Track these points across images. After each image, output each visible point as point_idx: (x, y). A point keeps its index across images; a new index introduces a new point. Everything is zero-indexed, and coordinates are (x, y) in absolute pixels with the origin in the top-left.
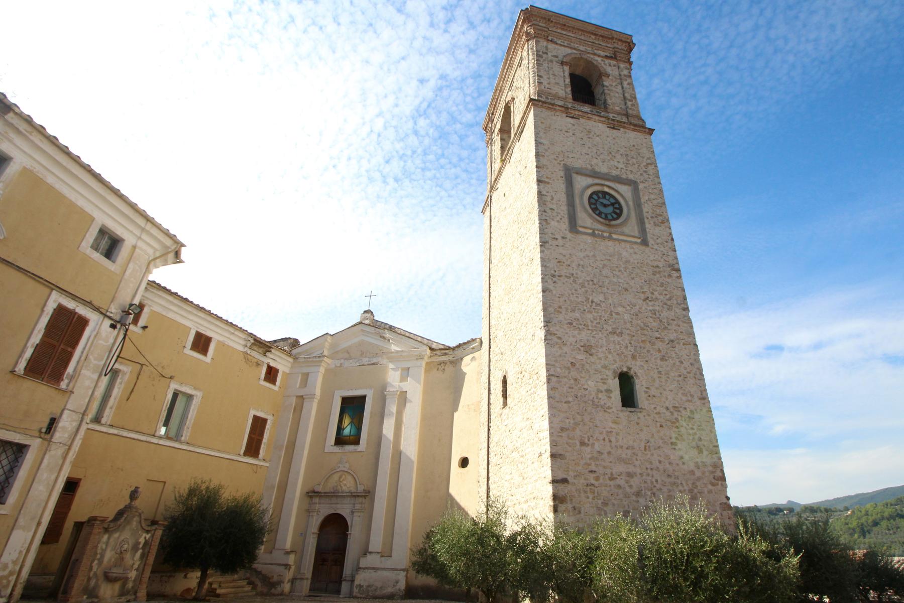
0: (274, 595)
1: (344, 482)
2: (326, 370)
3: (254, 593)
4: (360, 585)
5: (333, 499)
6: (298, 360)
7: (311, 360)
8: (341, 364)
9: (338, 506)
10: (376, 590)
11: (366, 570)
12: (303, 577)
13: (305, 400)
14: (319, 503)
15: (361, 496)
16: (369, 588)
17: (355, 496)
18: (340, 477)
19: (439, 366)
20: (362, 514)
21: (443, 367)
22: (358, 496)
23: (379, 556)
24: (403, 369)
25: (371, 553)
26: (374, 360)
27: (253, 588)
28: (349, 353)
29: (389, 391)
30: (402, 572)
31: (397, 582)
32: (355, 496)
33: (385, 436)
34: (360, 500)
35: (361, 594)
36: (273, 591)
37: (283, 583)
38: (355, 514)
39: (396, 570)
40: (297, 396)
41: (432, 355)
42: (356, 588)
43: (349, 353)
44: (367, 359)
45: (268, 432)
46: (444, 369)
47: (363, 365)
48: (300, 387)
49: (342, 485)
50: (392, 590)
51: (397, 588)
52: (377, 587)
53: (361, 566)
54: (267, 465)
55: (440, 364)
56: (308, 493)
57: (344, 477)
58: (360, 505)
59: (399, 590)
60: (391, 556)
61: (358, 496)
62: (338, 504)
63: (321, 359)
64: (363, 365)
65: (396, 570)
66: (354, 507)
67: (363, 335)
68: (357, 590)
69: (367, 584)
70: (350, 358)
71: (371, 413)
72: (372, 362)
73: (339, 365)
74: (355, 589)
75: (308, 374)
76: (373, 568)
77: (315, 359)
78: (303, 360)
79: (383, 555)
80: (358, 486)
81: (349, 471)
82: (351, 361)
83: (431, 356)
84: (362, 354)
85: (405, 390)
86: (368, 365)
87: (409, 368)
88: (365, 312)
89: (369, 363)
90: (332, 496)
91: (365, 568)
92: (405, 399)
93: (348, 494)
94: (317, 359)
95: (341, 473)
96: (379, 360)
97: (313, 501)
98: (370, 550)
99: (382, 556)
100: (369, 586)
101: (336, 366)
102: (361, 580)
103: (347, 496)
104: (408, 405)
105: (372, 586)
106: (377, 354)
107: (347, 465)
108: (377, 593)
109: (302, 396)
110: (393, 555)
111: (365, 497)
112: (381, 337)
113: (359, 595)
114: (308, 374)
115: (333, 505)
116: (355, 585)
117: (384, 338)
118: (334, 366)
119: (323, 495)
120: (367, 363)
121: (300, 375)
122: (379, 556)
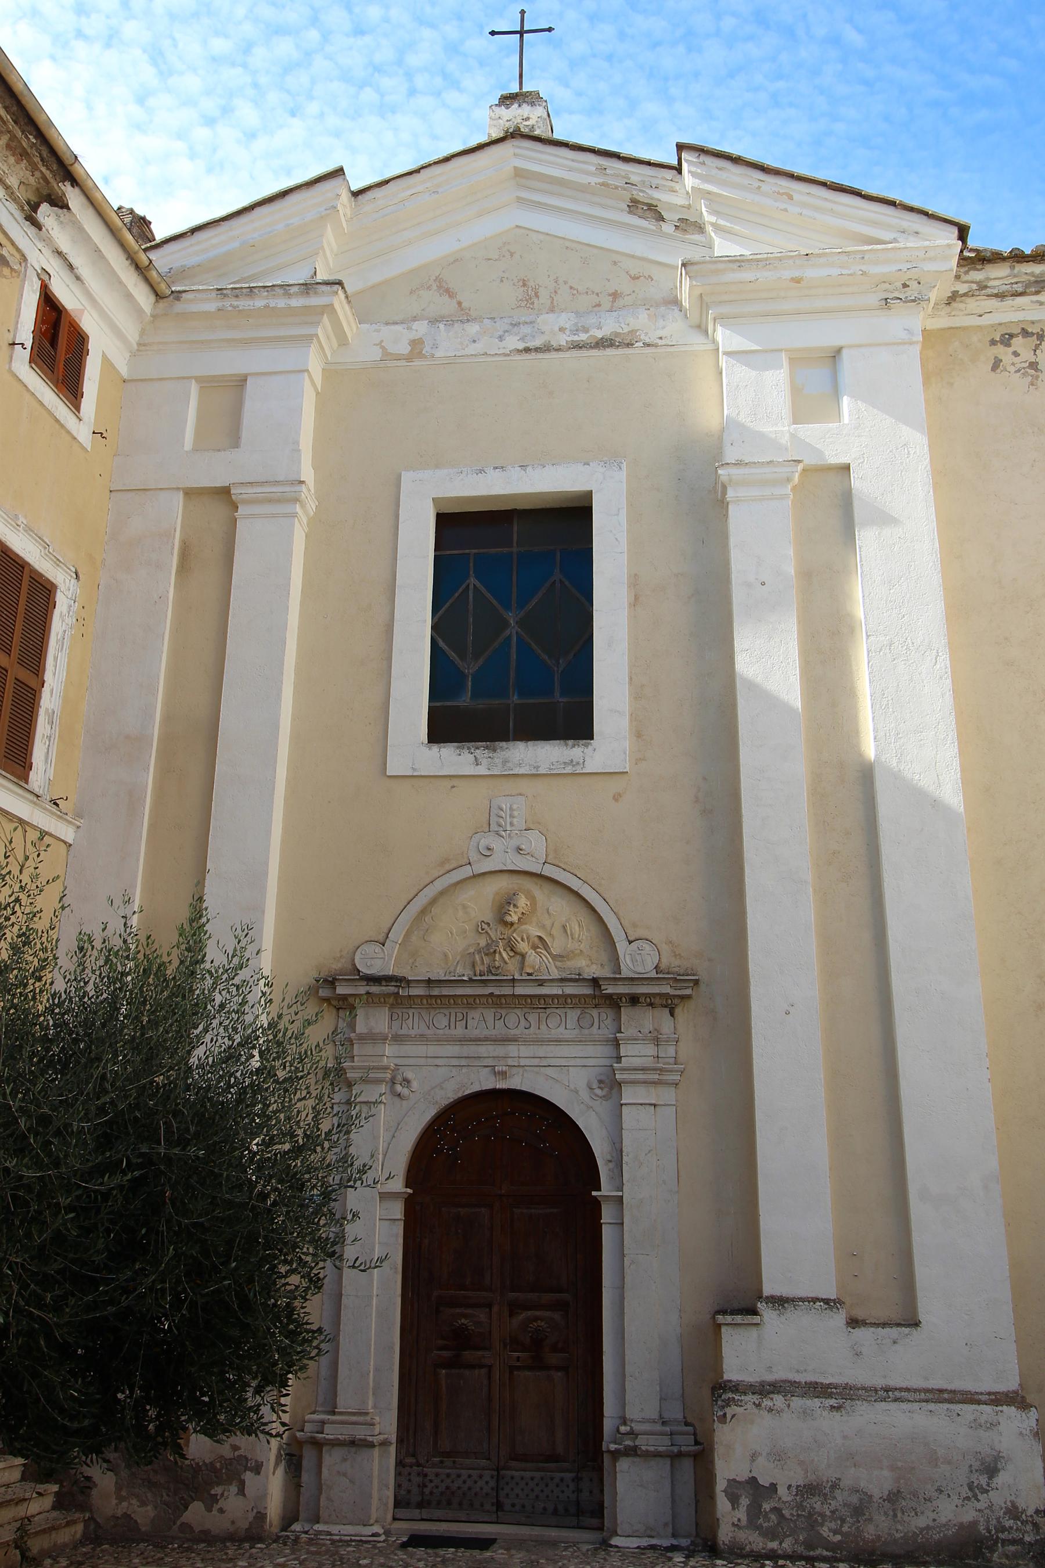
0: (207, 1538)
1: (534, 931)
2: (331, 373)
3: (79, 1528)
4: (753, 1481)
5: (475, 1015)
6: (179, 307)
7: (259, 303)
8: (416, 344)
9: (512, 1050)
10: (858, 1511)
11: (778, 1400)
12: (360, 1433)
13: (242, 510)
14: (398, 1039)
15: (651, 1002)
16: (816, 1503)
17: (614, 1002)
18: (506, 903)
19: (1000, 350)
20: (667, 1095)
21: (1027, 355)
22: (634, 1000)
23: (839, 1319)
24: (799, 359)
25: (780, 1302)
26: (608, 326)
27: (61, 1503)
28: (450, 293)
29: (739, 464)
30: (1010, 1411)
31: (991, 1470)
32: (614, 1002)
33: (752, 686)
34: (645, 1020)
35: (771, 1534)
36: (195, 1513)
37: (257, 1469)
38: (628, 1095)
39: (970, 1398)
40: (189, 493)
41: (962, 288)
42: (734, 1500)
43: (450, 293)
44: (565, 319)
45: (63, 659)
46: (1033, 365)
47: (546, 348)
48: (195, 449)
49: (523, 947)
50: (968, 1515)
51: (999, 1498)
52: (866, 1499)
53: (732, 1372)
54: (67, 833)
55: (1007, 339)
56: (331, 982)
57: (522, 901)
58: (650, 1050)
59: (1014, 1512)
60: (916, 1324)
61: (634, 1000)
62: (514, 1040)
63: (314, 301)
64: (546, 348)
65: (970, 1398)
66: (619, 1059)
67: (520, 200)
68: (741, 1514)
69: (798, 1478)
70: (463, 316)
71: (634, 581)
72: (599, 334)
73: (404, 349)
74: (723, 1504)
75: (241, 382)
76: (818, 1390)
77: (281, 303)
78: (211, 307)
79: (860, 1314)
80: (621, 946)
81: (549, 871)
82: (473, 329)
83: (954, 297)
84: (529, 296)
85: (834, 458)
86: (578, 346)
87: (836, 354)
88: (507, 100)
89: (583, 337)
90: (471, 1002)
91: (765, 1389)
92: (846, 502)
93: (570, 990)
94: (296, 302)
95: (503, 884)
96: (639, 321)
97: (361, 1027)
98: (768, 1290)
99: (854, 1323)
100: (810, 1489)
101: (387, 356)
102: (754, 1457)
103: (564, 1001)
104: (866, 538)
105: (835, 1486)
106: (615, 295)
107: (535, 842)
108: (870, 1532)
109: (224, 493)
110: (922, 1317)
111: (670, 1004)
112: (634, 205)
113: (756, 1541)
114: (241, 382)
115: (484, 1050)
116: (721, 1485)
117: (654, 212)
118: (376, 354)
119: (415, 991)
120: (563, 339)
121: (194, 389)
122: (839, 1319)
